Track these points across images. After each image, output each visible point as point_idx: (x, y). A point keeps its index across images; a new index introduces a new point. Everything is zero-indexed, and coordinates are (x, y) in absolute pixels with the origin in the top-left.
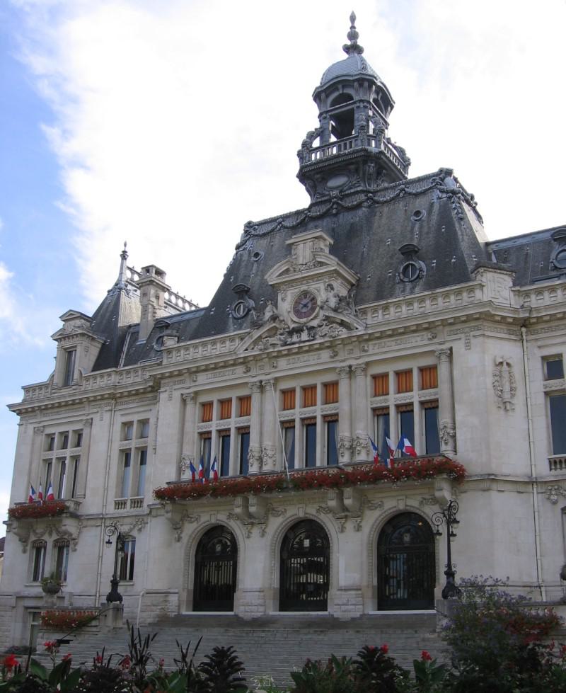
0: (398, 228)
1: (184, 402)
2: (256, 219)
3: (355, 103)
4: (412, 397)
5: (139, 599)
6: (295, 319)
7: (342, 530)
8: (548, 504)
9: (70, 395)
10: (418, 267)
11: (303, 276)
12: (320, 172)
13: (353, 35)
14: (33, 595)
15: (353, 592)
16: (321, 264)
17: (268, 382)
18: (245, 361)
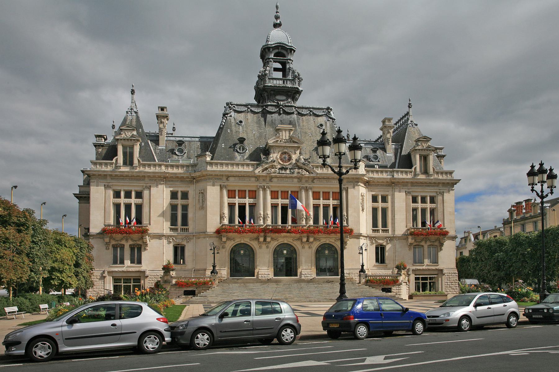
0: (313, 129)
3: (287, 60)
12: (274, 91)
13: (277, 18)
18: (257, 178)
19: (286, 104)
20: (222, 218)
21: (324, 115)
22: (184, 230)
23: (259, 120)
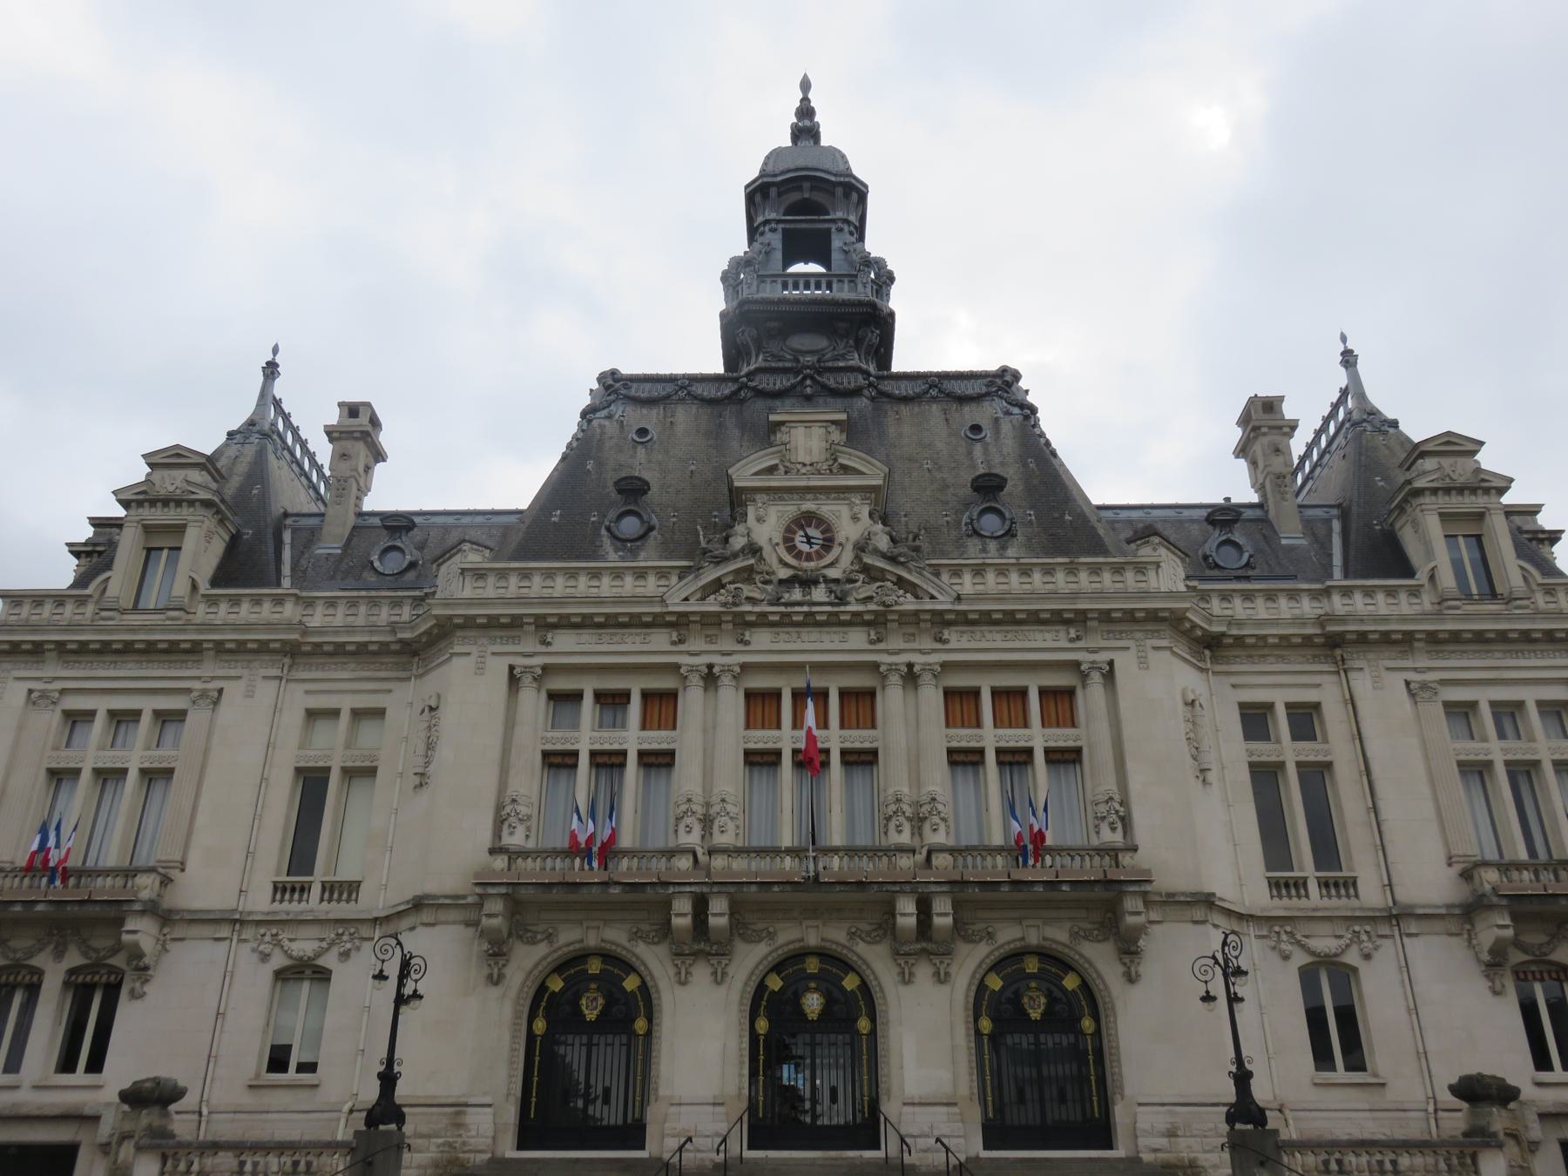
1: (514, 680)
2: (630, 366)
3: (833, 221)
4: (1030, 738)
5: (338, 1120)
6: (789, 559)
7: (907, 979)
8: (1274, 958)
9: (164, 629)
10: (1007, 515)
11: (812, 483)
14: (56, 1111)
15: (944, 1109)
16: (846, 469)
17: (727, 669)
18: (679, 624)
19: (830, 364)
20: (500, 822)
21: (988, 394)
22: (336, 896)
23: (720, 425)
